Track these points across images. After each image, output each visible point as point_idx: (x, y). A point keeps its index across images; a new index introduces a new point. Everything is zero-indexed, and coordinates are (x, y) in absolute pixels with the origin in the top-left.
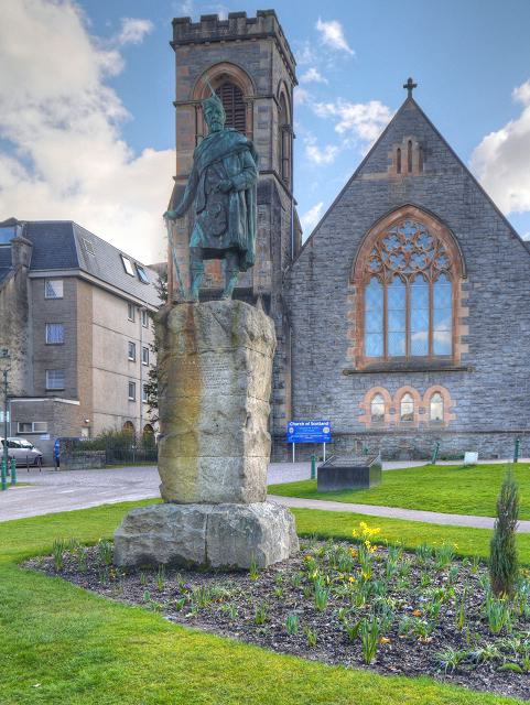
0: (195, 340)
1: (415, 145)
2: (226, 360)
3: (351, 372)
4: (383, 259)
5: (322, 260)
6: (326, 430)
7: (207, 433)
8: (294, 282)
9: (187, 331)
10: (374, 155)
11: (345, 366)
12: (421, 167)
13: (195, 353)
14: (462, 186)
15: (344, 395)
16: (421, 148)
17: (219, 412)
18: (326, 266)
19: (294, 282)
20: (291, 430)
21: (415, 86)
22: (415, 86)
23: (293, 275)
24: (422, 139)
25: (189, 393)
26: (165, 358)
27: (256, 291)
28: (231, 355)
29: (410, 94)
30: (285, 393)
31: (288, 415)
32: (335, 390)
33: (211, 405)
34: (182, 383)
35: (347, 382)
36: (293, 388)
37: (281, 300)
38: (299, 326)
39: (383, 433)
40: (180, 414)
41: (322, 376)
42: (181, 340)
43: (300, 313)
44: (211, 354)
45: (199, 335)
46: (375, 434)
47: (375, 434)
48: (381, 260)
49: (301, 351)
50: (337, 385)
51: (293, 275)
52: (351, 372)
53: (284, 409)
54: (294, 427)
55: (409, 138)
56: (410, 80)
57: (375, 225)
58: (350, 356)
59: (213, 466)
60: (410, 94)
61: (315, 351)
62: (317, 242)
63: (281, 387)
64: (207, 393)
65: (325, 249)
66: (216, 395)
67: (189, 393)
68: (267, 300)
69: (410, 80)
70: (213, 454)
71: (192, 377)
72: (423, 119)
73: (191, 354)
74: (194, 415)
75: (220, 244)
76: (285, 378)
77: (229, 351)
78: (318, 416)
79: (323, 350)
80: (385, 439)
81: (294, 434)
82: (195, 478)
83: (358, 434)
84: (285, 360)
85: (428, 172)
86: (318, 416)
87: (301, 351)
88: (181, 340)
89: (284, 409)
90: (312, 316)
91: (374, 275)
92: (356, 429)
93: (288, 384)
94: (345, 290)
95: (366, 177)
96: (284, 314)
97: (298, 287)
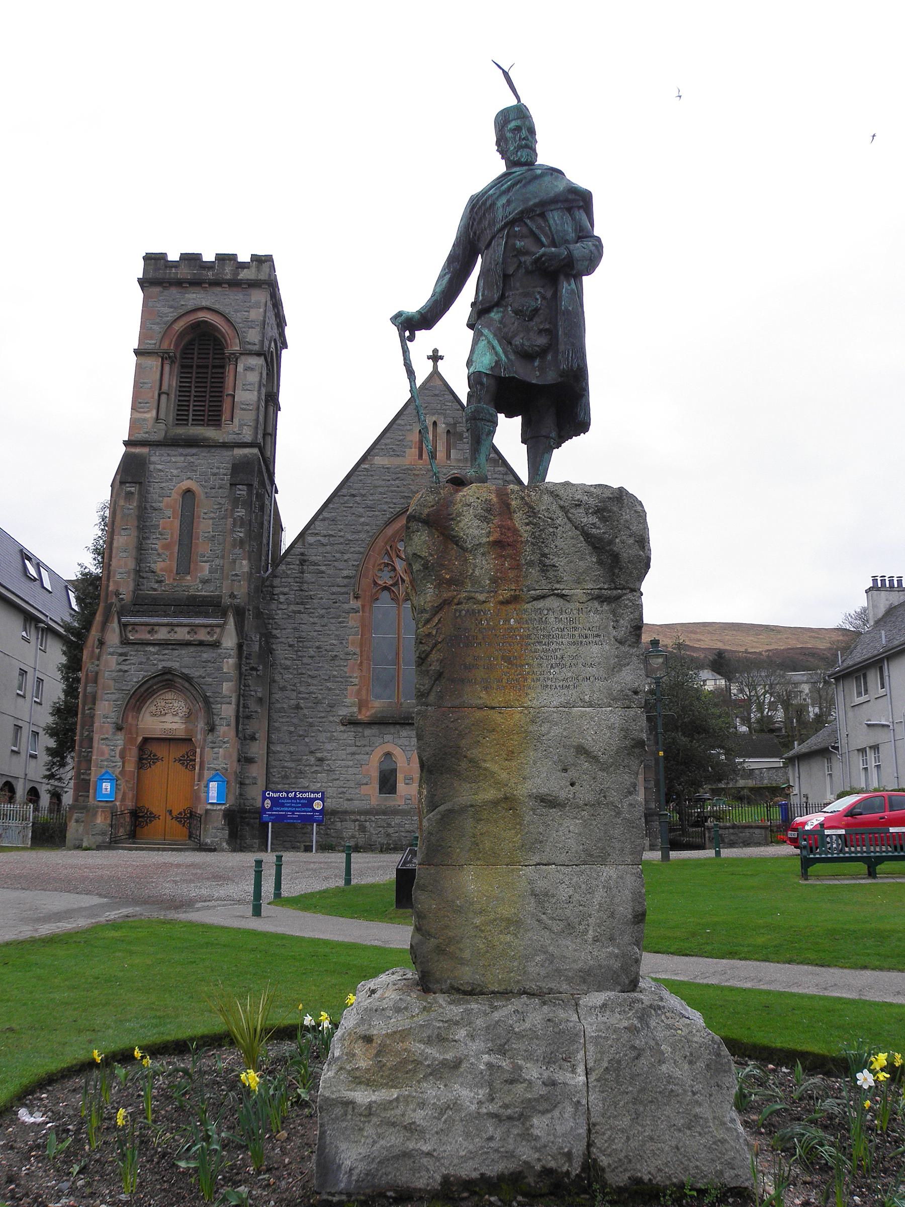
0: (518, 567)
1: (442, 427)
2: (595, 618)
3: (351, 722)
4: (398, 568)
5: (316, 564)
6: (318, 805)
7: (548, 802)
8: (276, 591)
9: (498, 544)
10: (388, 435)
11: (343, 712)
12: (448, 457)
13: (515, 599)
14: (500, 482)
15: (342, 754)
16: (448, 432)
17: (581, 750)
18: (323, 572)
19: (276, 591)
20: (268, 804)
21: (441, 358)
22: (441, 358)
23: (276, 582)
24: (451, 421)
25: (497, 698)
26: (438, 609)
27: (226, 601)
28: (606, 607)
29: (435, 367)
30: (257, 749)
31: (261, 782)
32: (328, 746)
33: (556, 731)
34: (480, 673)
35: (348, 736)
36: (269, 742)
37: (258, 615)
38: (282, 653)
39: (395, 812)
40: (474, 753)
41: (311, 725)
42: (483, 566)
43: (284, 635)
44: (553, 603)
45: (528, 554)
46: (384, 813)
47: (384, 813)
48: (394, 569)
49: (283, 689)
50: (331, 739)
51: (276, 582)
52: (351, 722)
53: (257, 771)
54: (271, 798)
55: (434, 419)
56: (435, 351)
57: (388, 523)
58: (351, 699)
59: (564, 892)
60: (435, 367)
61: (302, 689)
62: (311, 539)
63: (253, 738)
64: (546, 699)
65: (321, 549)
66: (568, 705)
67: (497, 698)
68: (240, 613)
69: (435, 351)
70: (563, 858)
71: (508, 660)
72: (451, 397)
73: (507, 602)
74: (510, 755)
75: (532, 374)
76: (259, 726)
77: (600, 599)
78: (305, 782)
79: (312, 688)
80: (397, 820)
81: (271, 809)
82: (514, 924)
83: (360, 813)
84: (260, 700)
85: (459, 461)
86: (305, 782)
87: (283, 689)
88: (483, 566)
89: (257, 771)
90: (300, 639)
91: (386, 588)
92: (357, 805)
93: (262, 735)
94: (346, 606)
95: (379, 461)
96: (262, 635)
97: (282, 598)
